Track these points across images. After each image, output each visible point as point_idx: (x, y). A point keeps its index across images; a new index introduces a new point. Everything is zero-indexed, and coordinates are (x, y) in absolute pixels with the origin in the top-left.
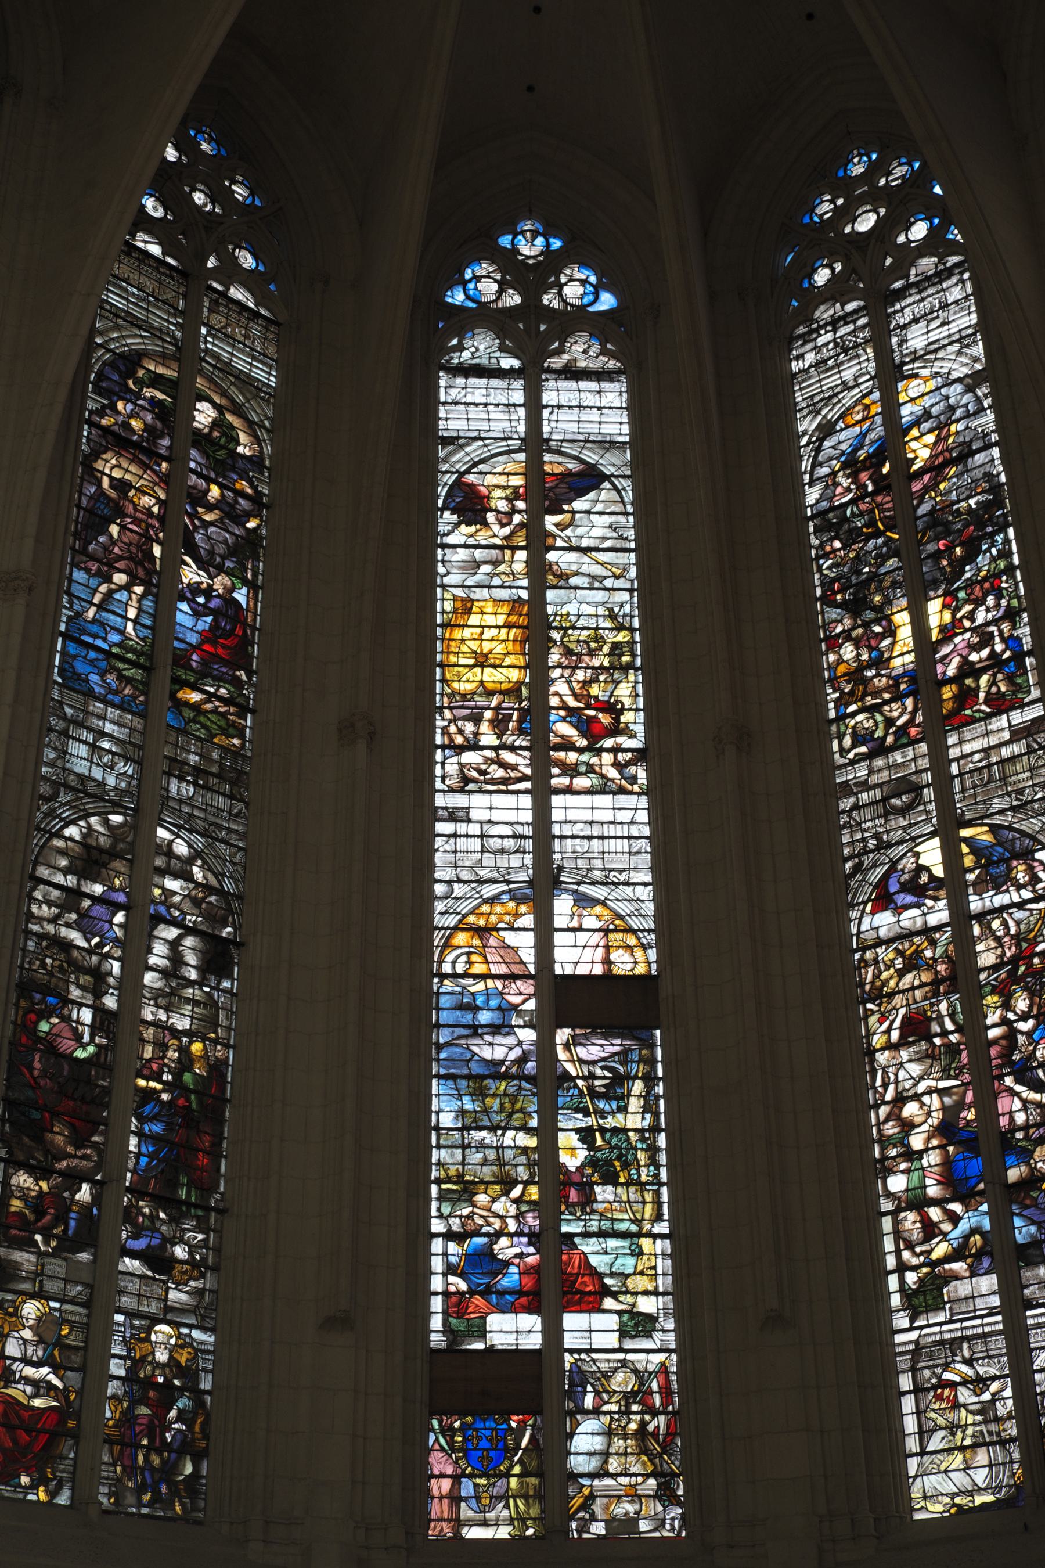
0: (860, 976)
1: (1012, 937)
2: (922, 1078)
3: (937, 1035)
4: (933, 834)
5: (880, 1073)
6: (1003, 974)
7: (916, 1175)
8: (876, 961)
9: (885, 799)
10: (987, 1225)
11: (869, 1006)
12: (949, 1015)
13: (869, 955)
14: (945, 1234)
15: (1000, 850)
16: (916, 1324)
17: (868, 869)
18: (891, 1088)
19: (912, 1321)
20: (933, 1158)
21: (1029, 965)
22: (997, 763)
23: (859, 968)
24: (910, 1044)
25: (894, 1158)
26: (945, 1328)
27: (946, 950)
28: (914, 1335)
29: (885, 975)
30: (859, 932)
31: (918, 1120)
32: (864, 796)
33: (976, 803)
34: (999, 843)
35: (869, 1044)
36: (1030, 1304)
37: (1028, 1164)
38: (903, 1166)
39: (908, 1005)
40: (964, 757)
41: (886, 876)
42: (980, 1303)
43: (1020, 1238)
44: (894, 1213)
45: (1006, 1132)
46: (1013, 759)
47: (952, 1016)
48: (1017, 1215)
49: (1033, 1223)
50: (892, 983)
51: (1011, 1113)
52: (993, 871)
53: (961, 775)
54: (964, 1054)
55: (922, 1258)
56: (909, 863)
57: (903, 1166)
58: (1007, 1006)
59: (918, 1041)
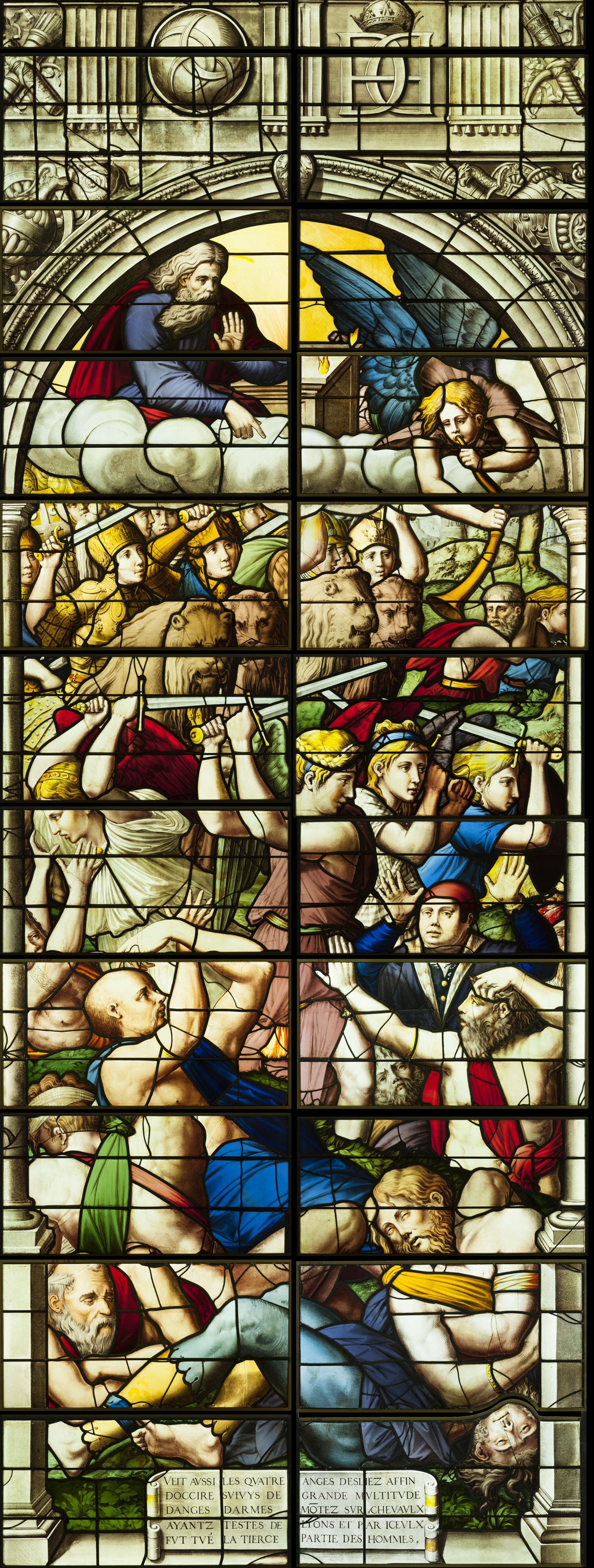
5: (42, 866)
11: (32, 667)
18: (69, 918)
29: (88, 591)
31: (131, 1026)
38: (81, 1141)
39: (141, 694)
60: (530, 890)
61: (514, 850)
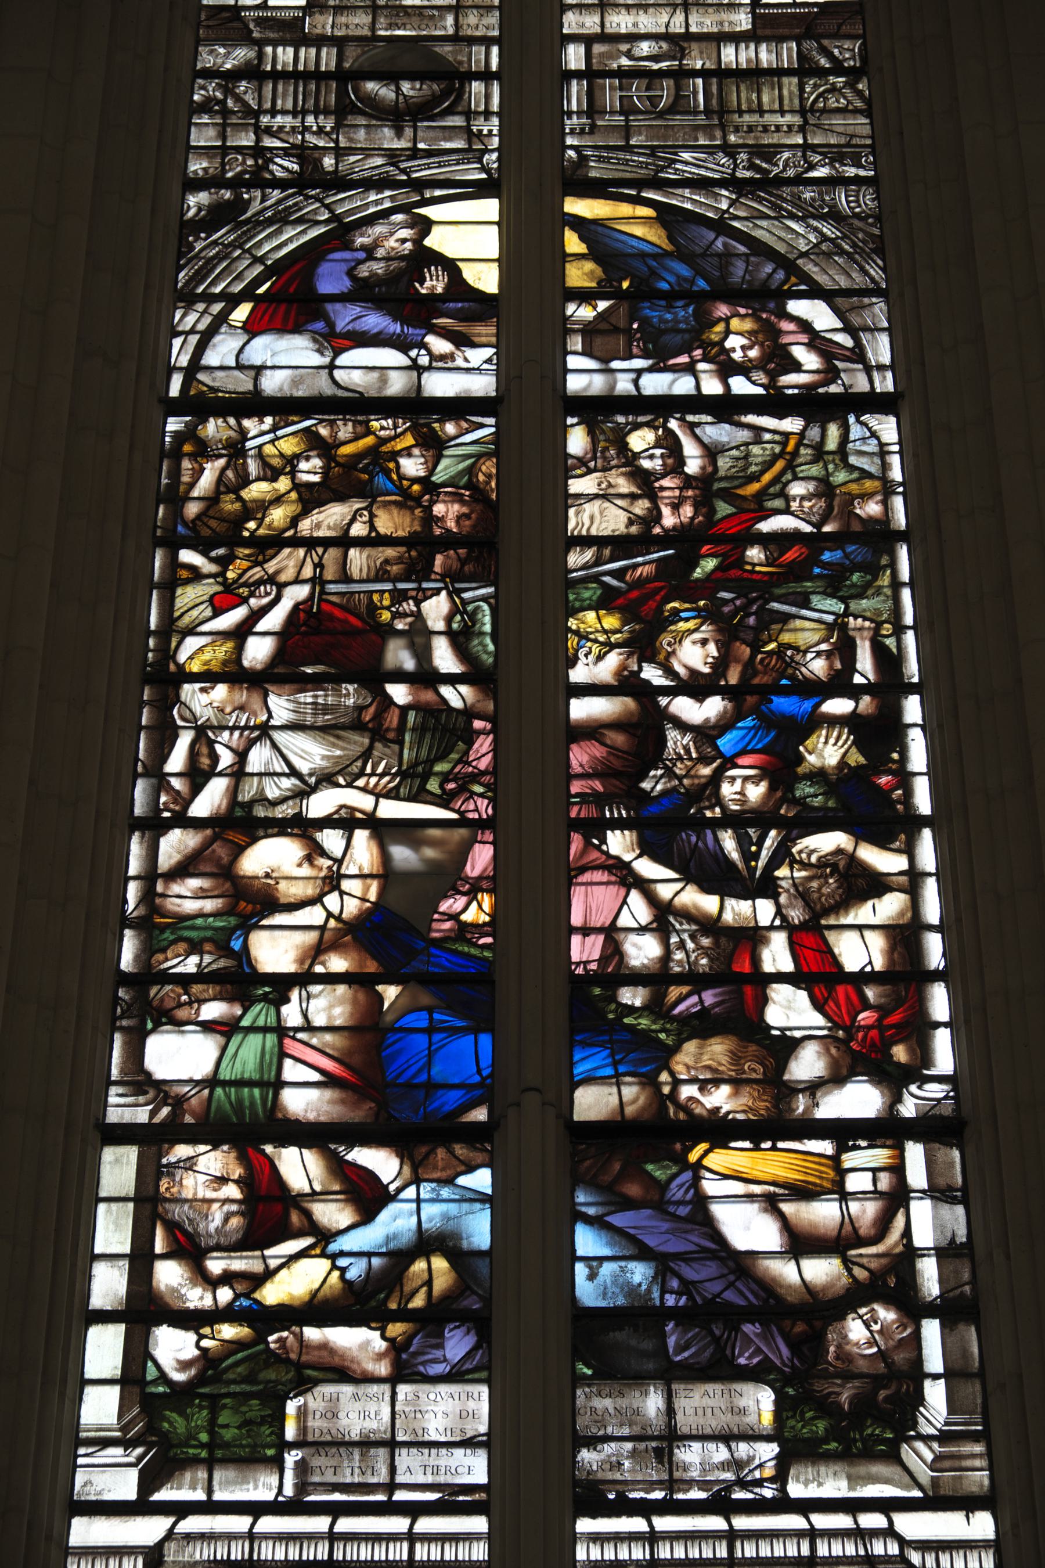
0: (175, 473)
1: (688, 481)
2: (326, 779)
3: (399, 676)
4: (479, 190)
5: (184, 741)
6: (644, 565)
7: (249, 1053)
8: (236, 449)
9: (342, 76)
10: (479, 1230)
12: (449, 633)
13: (213, 428)
14: (324, 1237)
15: (684, 271)
16: (164, 1495)
17: (258, 223)
19: (149, 1482)
20: (328, 1006)
21: (732, 561)
22: (704, 73)
23: (176, 455)
24: (305, 683)
25: (185, 981)
26: (268, 1524)
27: (471, 471)
28: (148, 1530)
30: (195, 365)
32: (285, 55)
33: (628, 148)
34: (681, 254)
35: (167, 654)
36: (596, 1499)
37: (650, 1081)
40: (604, 37)
41: (310, 256)
42: (411, 1467)
43: (587, 1291)
44: (152, 1140)
45: (589, 979)
46: (754, 75)
47: (460, 640)
48: (589, 1220)
49: (643, 1253)
50: (278, 516)
51: (611, 933)
52: (653, 313)
53: (590, 74)
54: (483, 745)
55: (225, 1295)
56: (395, 238)
57: (213, 1010)
58: (644, 644)
59: (336, 680)
60: (856, 758)
61: (833, 721)
